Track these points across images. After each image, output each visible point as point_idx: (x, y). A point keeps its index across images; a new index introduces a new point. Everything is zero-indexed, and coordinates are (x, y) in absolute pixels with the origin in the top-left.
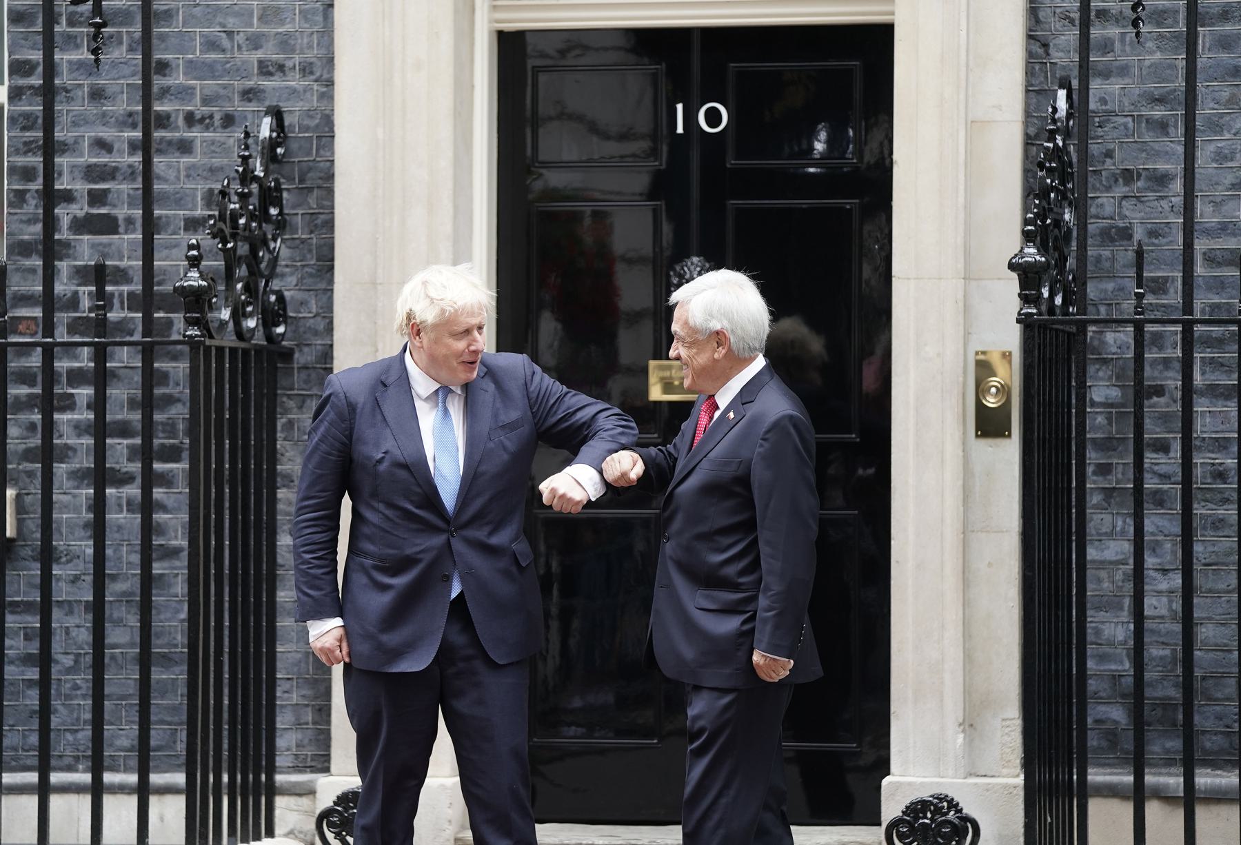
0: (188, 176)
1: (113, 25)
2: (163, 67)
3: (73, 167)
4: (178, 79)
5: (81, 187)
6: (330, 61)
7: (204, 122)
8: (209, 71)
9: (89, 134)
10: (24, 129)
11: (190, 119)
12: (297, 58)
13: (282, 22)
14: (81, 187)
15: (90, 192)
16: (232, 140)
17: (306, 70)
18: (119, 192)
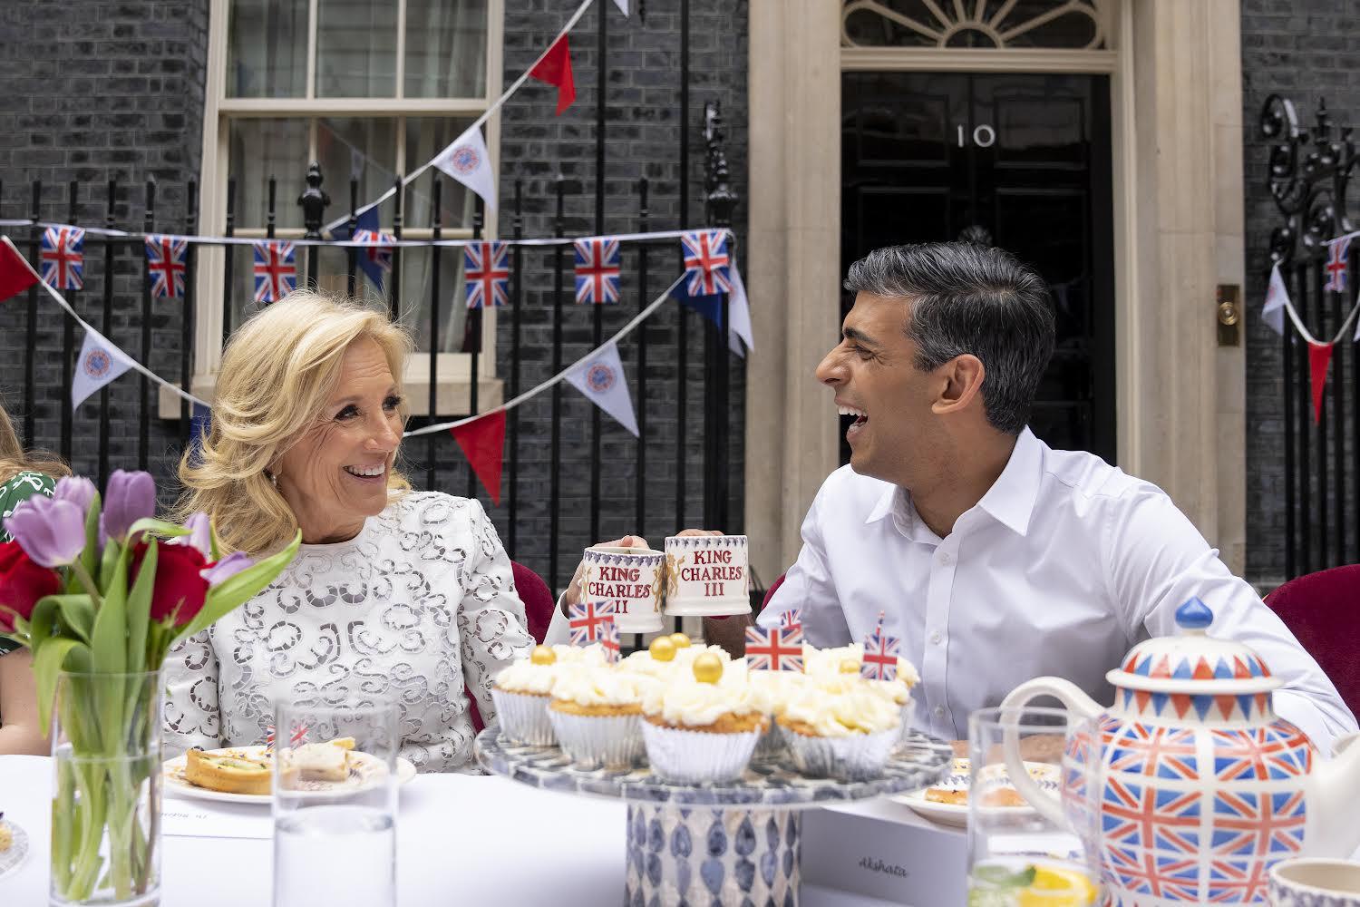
0: (635, 154)
1: (580, 45)
2: (617, 76)
3: (549, 146)
4: (629, 84)
5: (555, 160)
6: (744, 71)
7: (649, 115)
8: (652, 79)
9: (561, 123)
10: (514, 118)
11: (637, 113)
12: (717, 72)
13: (706, 46)
14: (555, 160)
15: (562, 164)
16: (667, 129)
17: (724, 79)
18: (583, 165)
